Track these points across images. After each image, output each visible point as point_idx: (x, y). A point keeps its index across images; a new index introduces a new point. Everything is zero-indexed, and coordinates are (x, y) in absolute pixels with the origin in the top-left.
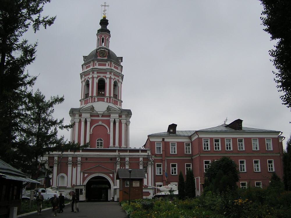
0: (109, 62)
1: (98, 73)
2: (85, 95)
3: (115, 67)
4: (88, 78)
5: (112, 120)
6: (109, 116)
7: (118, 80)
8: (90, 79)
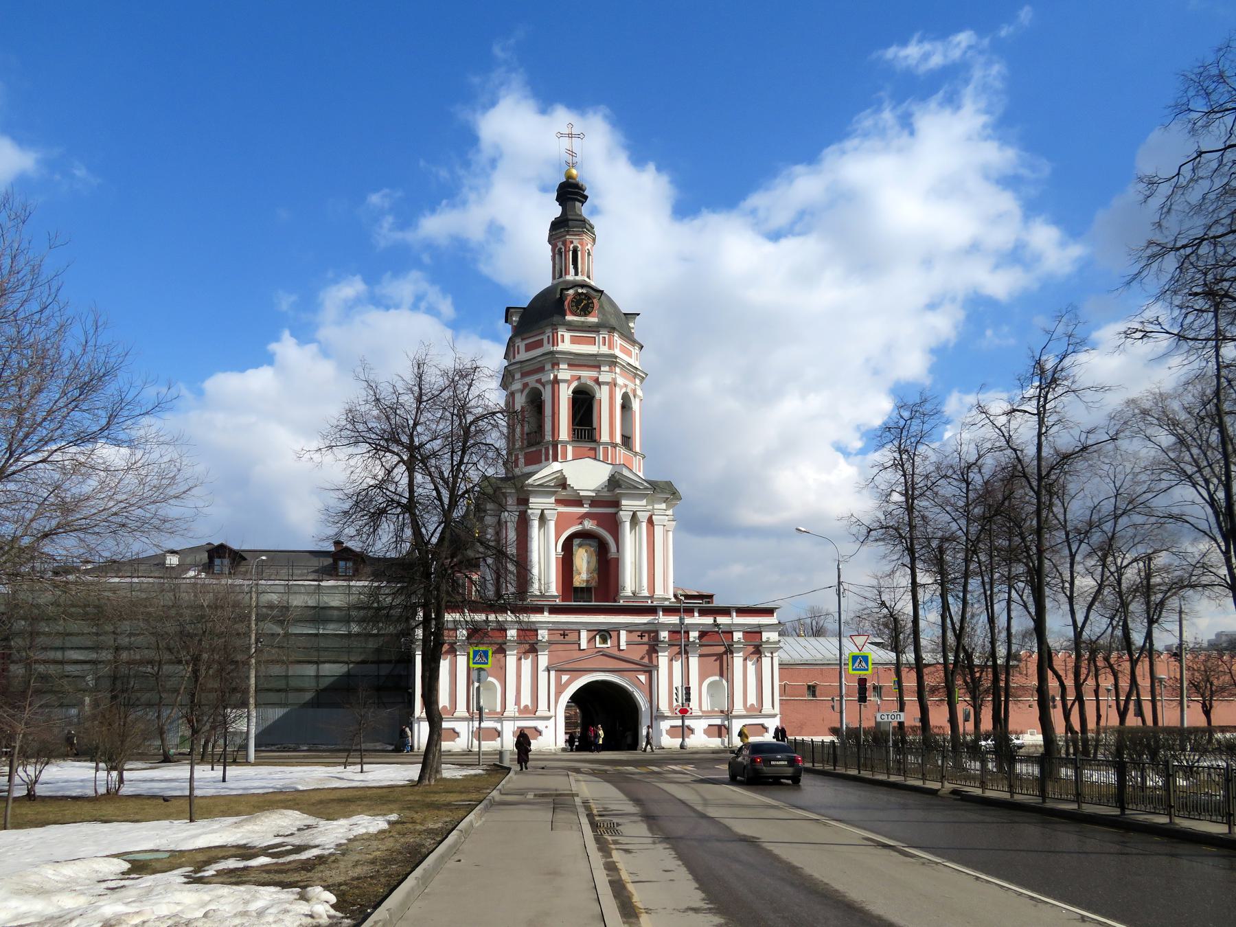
0: (604, 334)
1: (572, 365)
2: (525, 437)
3: (623, 349)
4: (539, 381)
5: (625, 516)
6: (616, 504)
7: (634, 391)
8: (544, 386)
